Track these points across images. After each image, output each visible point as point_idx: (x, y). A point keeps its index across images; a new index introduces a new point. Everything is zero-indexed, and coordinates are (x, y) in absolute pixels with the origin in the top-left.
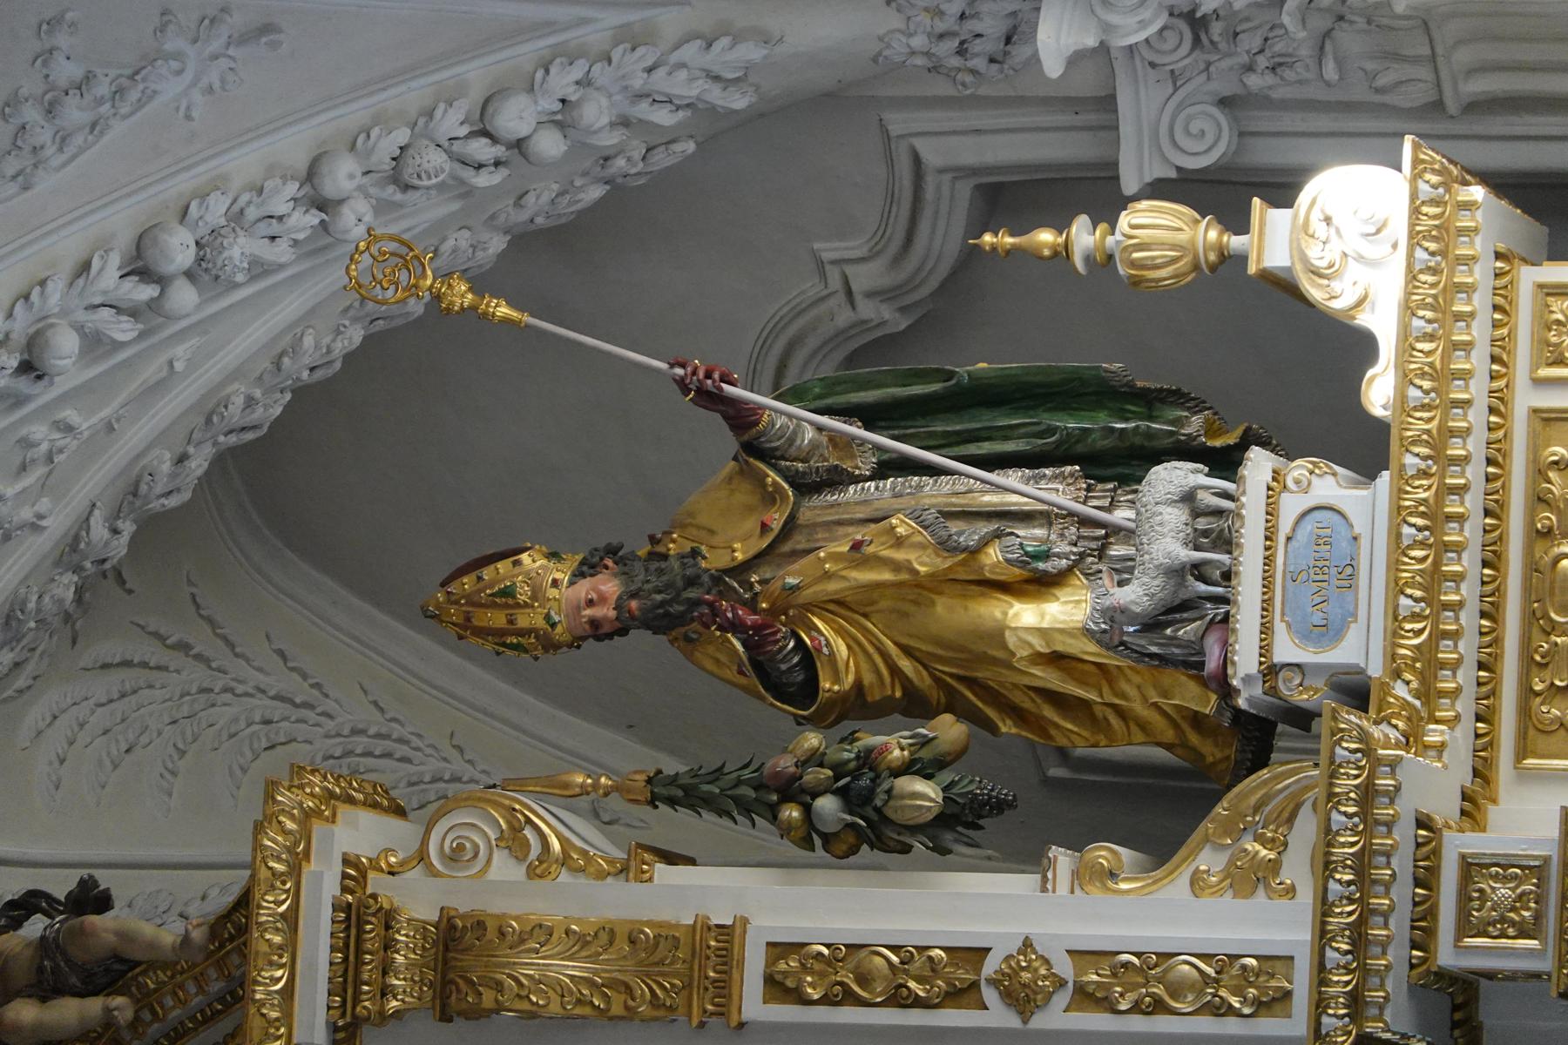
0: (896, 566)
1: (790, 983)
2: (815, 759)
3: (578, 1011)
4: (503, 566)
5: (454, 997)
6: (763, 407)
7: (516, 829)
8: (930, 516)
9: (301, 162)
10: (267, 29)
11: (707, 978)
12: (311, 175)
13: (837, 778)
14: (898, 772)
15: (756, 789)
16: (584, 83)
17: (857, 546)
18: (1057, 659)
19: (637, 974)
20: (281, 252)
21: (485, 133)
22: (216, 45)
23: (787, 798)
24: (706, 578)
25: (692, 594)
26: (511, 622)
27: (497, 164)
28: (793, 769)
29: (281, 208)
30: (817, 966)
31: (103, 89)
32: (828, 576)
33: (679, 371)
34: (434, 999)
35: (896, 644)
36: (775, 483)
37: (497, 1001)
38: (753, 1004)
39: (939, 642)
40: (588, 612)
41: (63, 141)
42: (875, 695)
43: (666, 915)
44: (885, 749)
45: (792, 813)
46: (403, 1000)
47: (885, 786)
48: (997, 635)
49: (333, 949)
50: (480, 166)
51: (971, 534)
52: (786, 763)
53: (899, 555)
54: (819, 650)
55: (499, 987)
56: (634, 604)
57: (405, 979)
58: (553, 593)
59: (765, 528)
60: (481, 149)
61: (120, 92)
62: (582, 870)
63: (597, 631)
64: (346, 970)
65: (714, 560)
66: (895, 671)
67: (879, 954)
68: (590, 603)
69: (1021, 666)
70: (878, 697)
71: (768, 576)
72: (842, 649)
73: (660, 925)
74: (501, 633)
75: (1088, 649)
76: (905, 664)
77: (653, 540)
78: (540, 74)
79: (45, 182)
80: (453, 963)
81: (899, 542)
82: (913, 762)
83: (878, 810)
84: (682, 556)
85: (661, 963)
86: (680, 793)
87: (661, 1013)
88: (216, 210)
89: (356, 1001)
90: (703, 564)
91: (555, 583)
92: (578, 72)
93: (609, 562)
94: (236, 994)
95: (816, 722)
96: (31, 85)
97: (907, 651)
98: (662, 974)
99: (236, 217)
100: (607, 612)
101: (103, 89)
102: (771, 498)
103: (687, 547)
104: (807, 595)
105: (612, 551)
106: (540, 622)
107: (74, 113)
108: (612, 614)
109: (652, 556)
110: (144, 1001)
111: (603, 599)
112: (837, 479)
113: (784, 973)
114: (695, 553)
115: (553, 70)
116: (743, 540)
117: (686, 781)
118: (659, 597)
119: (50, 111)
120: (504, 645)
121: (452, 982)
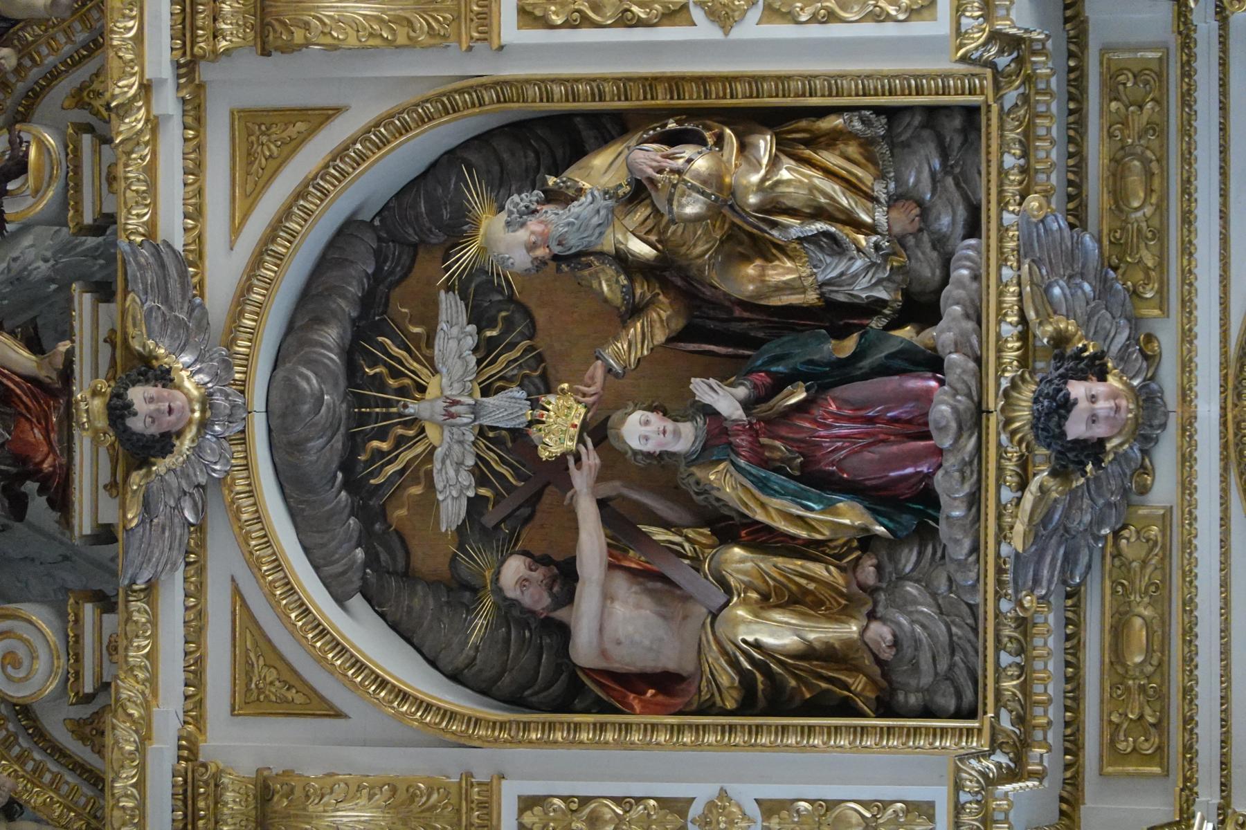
1: (538, 12)
3: (371, 42)
5: (271, 37)
11: (472, 11)
19: (416, 11)
34: (255, 38)
37: (305, 37)
38: (509, 30)
46: (231, 41)
55: (307, 26)
57: (231, 24)
64: (184, 19)
67: (607, 806)
80: (269, 9)
87: (436, 41)
89: (193, 43)
94: (97, 43)
98: (436, 10)
110: (24, 51)
121: (269, 24)
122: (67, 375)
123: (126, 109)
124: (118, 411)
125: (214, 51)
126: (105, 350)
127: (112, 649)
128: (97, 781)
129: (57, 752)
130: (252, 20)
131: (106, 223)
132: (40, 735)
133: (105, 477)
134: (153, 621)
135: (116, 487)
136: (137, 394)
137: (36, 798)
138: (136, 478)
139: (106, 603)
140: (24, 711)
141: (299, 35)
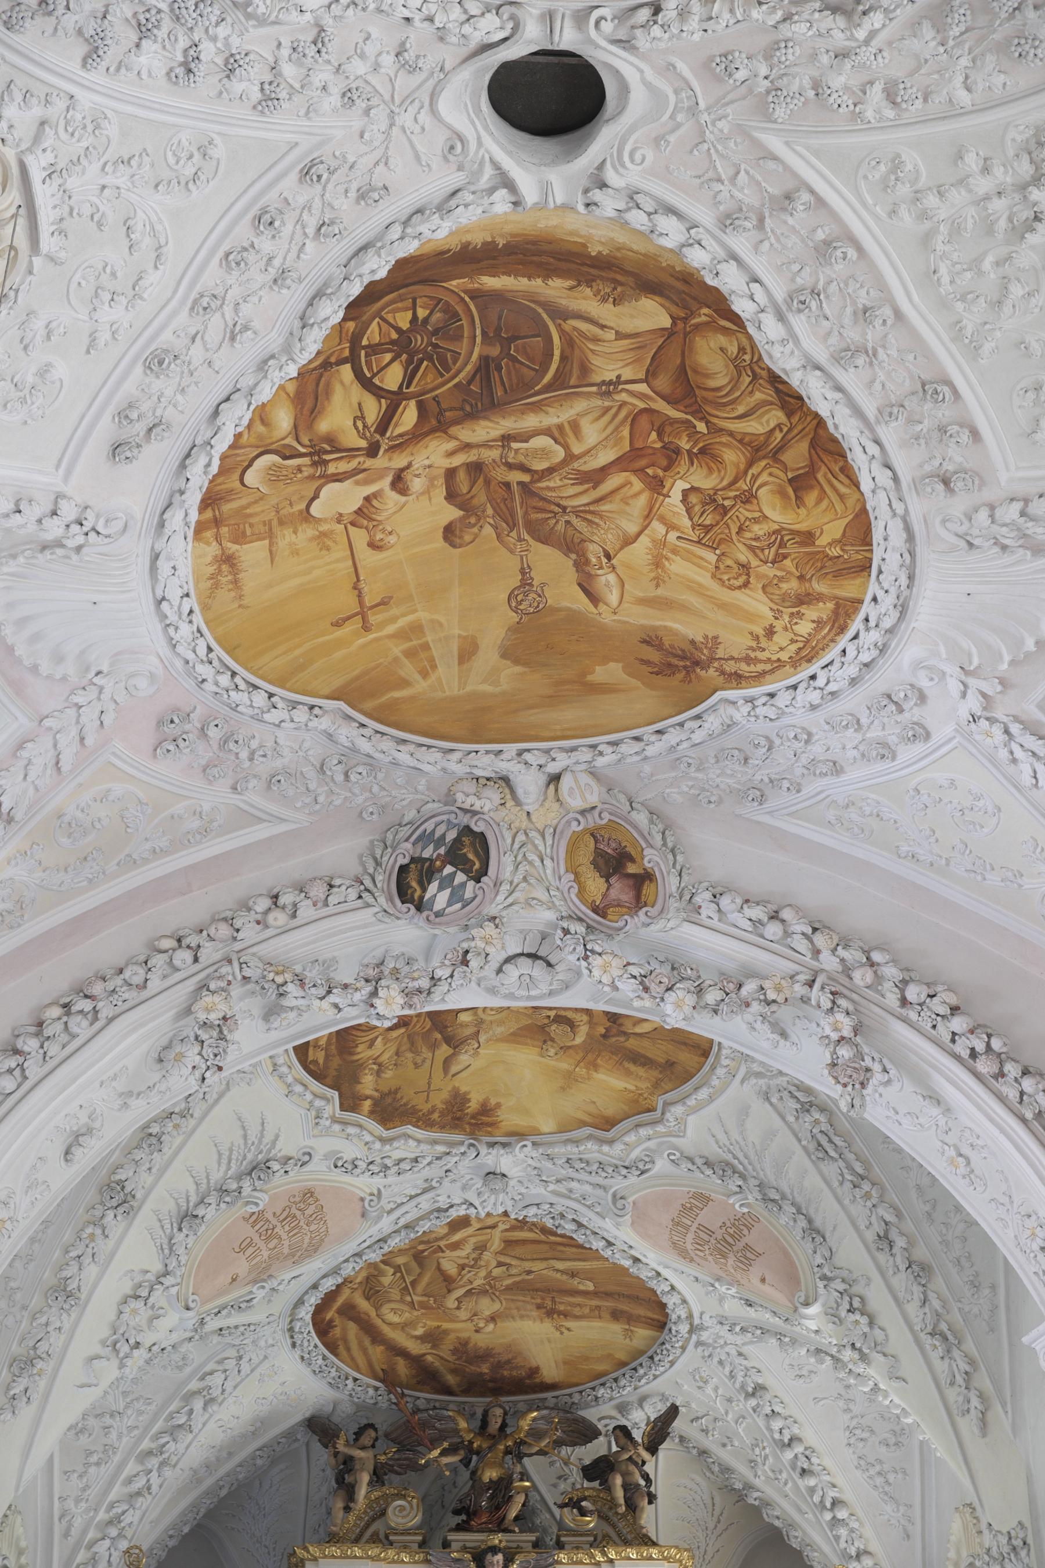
9: (870, 1549)
10: (908, 1536)
12: (867, 1552)
20: (843, 1545)
22: (902, 1522)
29: (856, 1544)
31: (887, 1489)
41: (870, 1478)
61: (886, 1494)
79: (858, 1473)
88: (855, 1525)
94: (627, 1543)
96: (886, 1467)
99: (852, 1531)
101: (887, 1489)
107: (879, 1481)
110: (624, 1516)
119: (879, 1473)
122: (506, 1531)
123: (604, 1554)
124: (494, 1550)
126: (514, 1545)
127: (405, 1547)
128: (356, 1541)
129: (368, 1526)
131: (560, 1546)
132: (373, 1519)
133: (468, 1545)
134: (415, 1562)
135: (464, 1549)
136: (500, 1557)
137: (351, 1518)
138: (468, 1556)
139: (422, 1545)
140: (383, 1513)
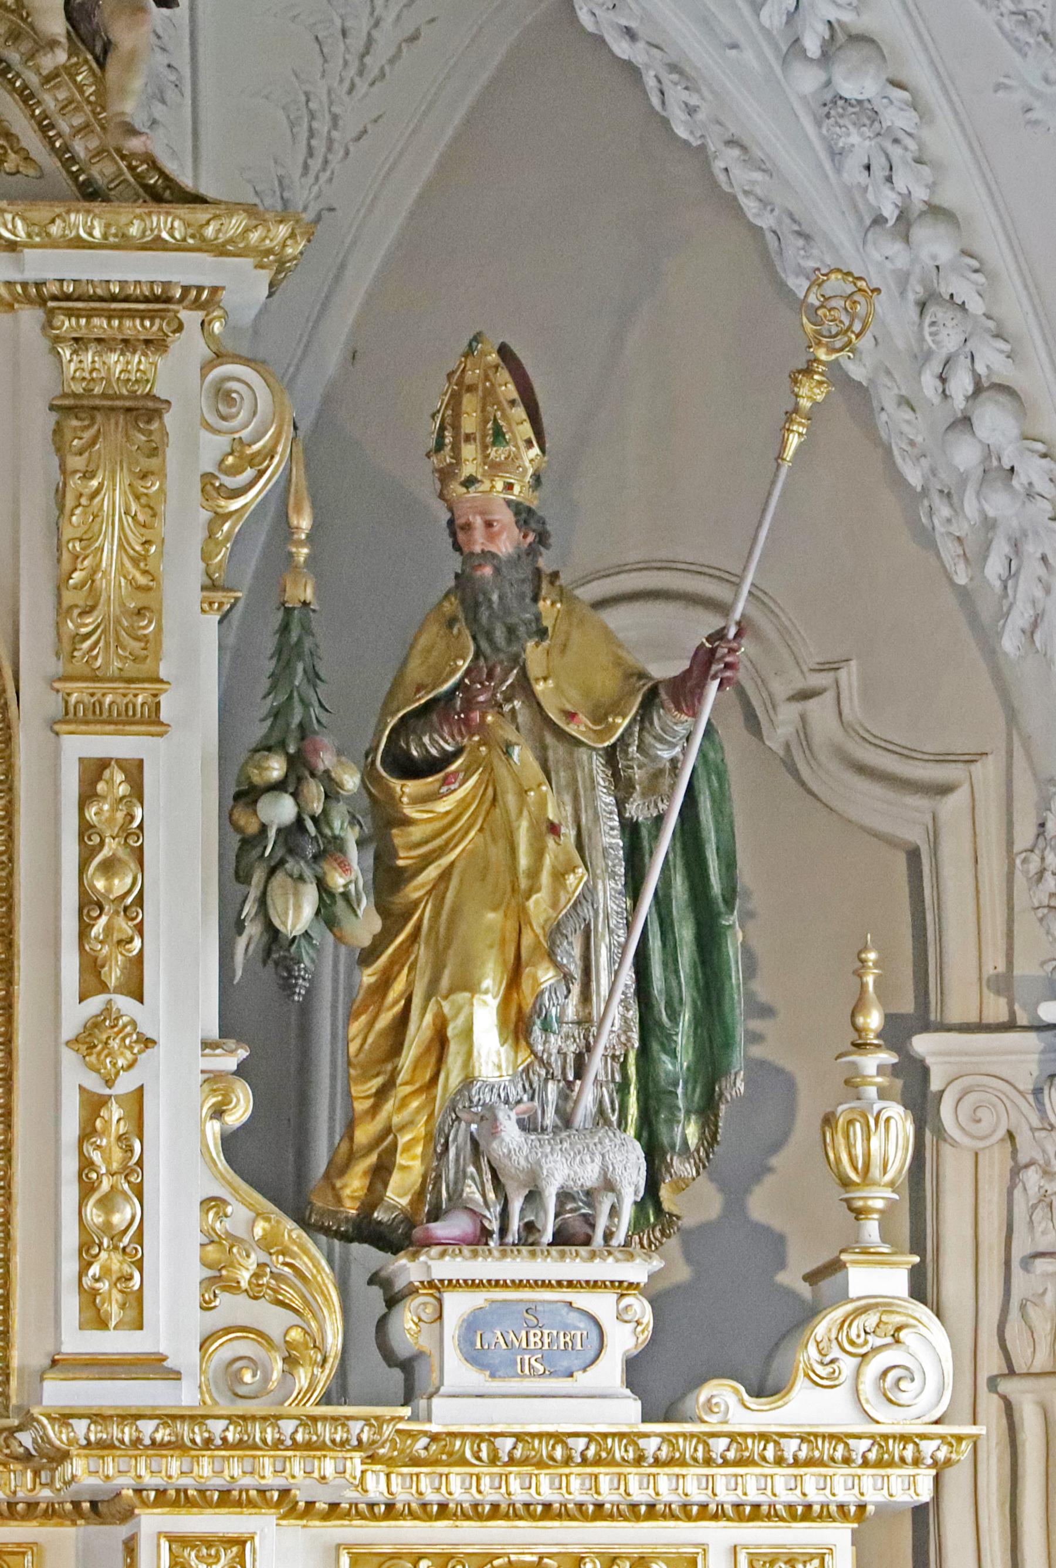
0: (534, 873)
1: (101, 787)
2: (331, 795)
3: (66, 557)
4: (526, 430)
5: (75, 423)
6: (695, 714)
7: (252, 460)
8: (587, 911)
11: (104, 695)
13: (314, 819)
14: (322, 886)
15: (301, 726)
16: (1030, 494)
17: (554, 829)
18: (440, 1041)
19: (106, 618)
21: (978, 389)
23: (292, 762)
24: (514, 649)
25: (500, 634)
26: (468, 438)
27: (945, 395)
28: (321, 767)
30: (120, 816)
32: (522, 793)
33: (732, 632)
34: (75, 395)
35: (452, 864)
36: (616, 726)
37: (75, 472)
39: (456, 912)
40: (478, 522)
42: (399, 837)
43: (169, 643)
44: (344, 867)
45: (276, 768)
46: (70, 361)
47: (308, 873)
48: (467, 984)
49: (123, 284)
50: (943, 379)
51: (571, 955)
52: (326, 760)
53: (545, 878)
54: (445, 781)
55: (88, 475)
56: (488, 571)
57: (93, 362)
58: (499, 485)
59: (571, 716)
60: (961, 384)
62: (211, 535)
63: (456, 529)
64: (101, 299)
65: (534, 654)
66: (426, 861)
68: (489, 524)
69: (432, 1007)
70: (397, 841)
71: (520, 719)
72: (443, 806)
73: (159, 643)
74: (456, 427)
75: (453, 1075)
76: (432, 872)
77: (555, 575)
78: (1040, 447)
80: (113, 421)
81: (559, 876)
82: (332, 895)
83: (282, 862)
84: (538, 618)
85: (119, 644)
86: (294, 637)
87: (66, 646)
89: (70, 313)
90: (530, 644)
91: (509, 487)
92: (1042, 486)
93: (531, 538)
95: (369, 775)
97: (445, 875)
98: (107, 644)
100: (479, 543)
102: (601, 715)
103: (547, 622)
104: (501, 770)
105: (542, 538)
106: (468, 469)
108: (478, 549)
109: (538, 573)
111: (491, 538)
112: (622, 788)
113: (110, 782)
114: (542, 633)
115: (1044, 462)
116: (557, 687)
117: (308, 643)
118: (495, 597)
120: (442, 428)
121: (93, 420)
125: (57, 340)
130: (98, 390)
141: (76, 462)
